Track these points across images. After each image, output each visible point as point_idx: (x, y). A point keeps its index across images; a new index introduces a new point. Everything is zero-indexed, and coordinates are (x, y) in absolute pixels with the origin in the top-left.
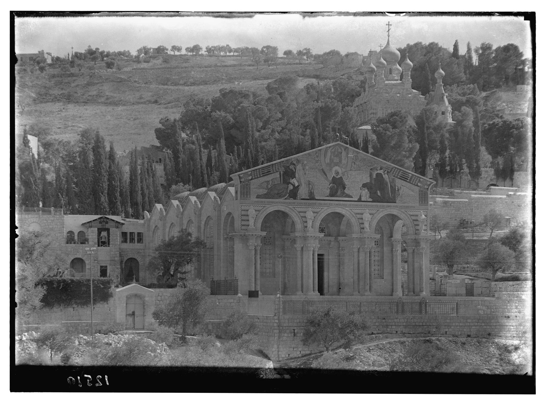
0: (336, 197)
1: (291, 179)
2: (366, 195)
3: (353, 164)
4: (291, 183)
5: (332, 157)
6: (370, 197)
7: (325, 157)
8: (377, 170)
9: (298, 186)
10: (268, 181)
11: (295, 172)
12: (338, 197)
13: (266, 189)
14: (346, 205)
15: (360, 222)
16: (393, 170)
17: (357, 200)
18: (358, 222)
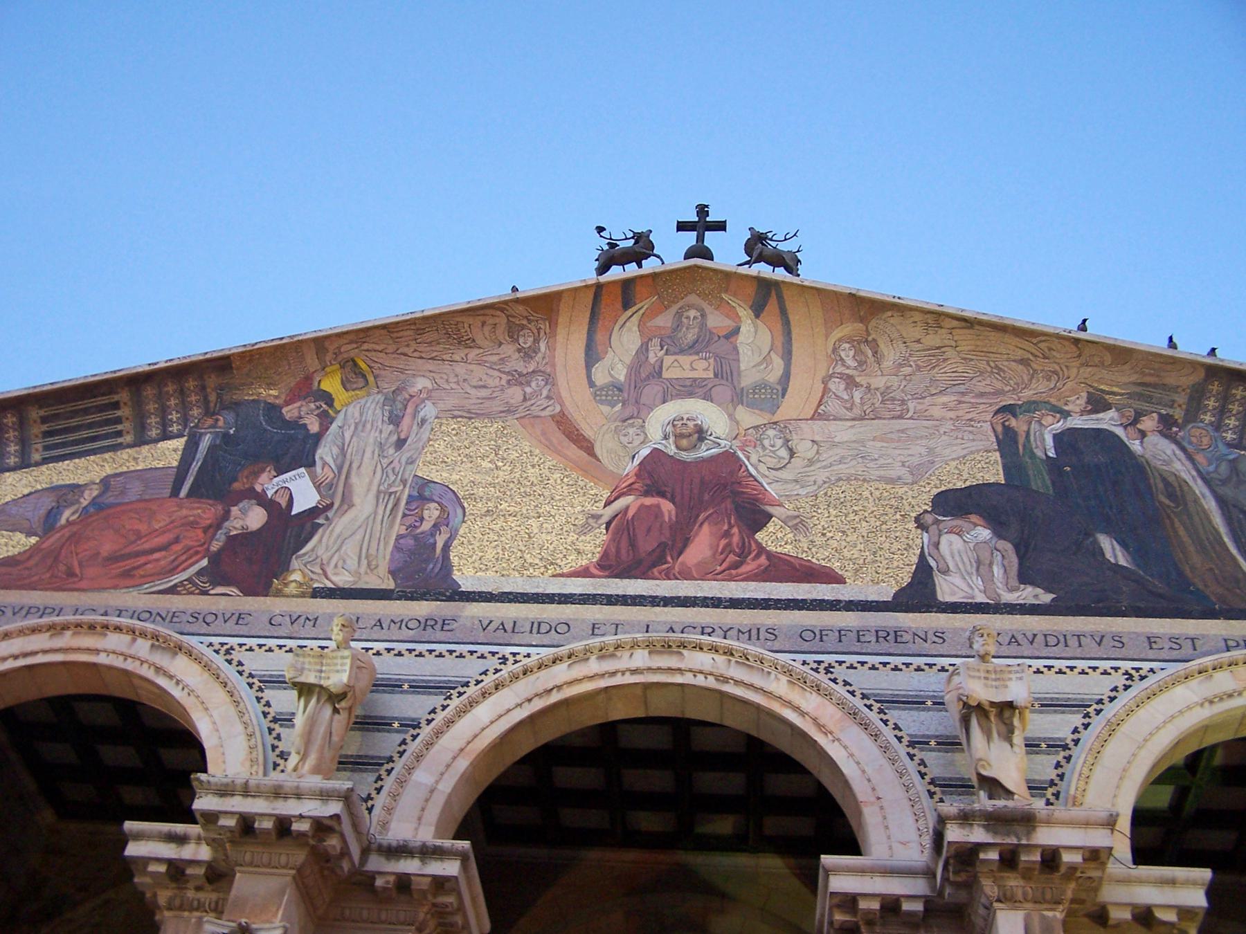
0: (668, 576)
1: (264, 477)
2: (982, 567)
3: (837, 386)
4: (262, 500)
5: (654, 354)
6: (1025, 578)
7: (591, 356)
8: (1066, 414)
9: (313, 512)
10: (76, 489)
11: (318, 437)
12: (686, 575)
13: (29, 534)
14: (771, 631)
15: (934, 771)
16: (1211, 403)
17: (886, 592)
18: (912, 767)
